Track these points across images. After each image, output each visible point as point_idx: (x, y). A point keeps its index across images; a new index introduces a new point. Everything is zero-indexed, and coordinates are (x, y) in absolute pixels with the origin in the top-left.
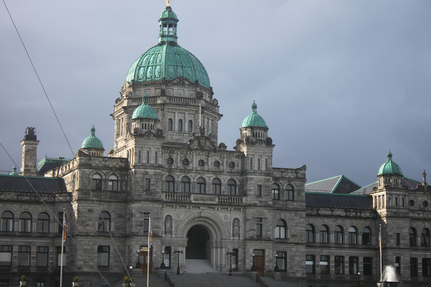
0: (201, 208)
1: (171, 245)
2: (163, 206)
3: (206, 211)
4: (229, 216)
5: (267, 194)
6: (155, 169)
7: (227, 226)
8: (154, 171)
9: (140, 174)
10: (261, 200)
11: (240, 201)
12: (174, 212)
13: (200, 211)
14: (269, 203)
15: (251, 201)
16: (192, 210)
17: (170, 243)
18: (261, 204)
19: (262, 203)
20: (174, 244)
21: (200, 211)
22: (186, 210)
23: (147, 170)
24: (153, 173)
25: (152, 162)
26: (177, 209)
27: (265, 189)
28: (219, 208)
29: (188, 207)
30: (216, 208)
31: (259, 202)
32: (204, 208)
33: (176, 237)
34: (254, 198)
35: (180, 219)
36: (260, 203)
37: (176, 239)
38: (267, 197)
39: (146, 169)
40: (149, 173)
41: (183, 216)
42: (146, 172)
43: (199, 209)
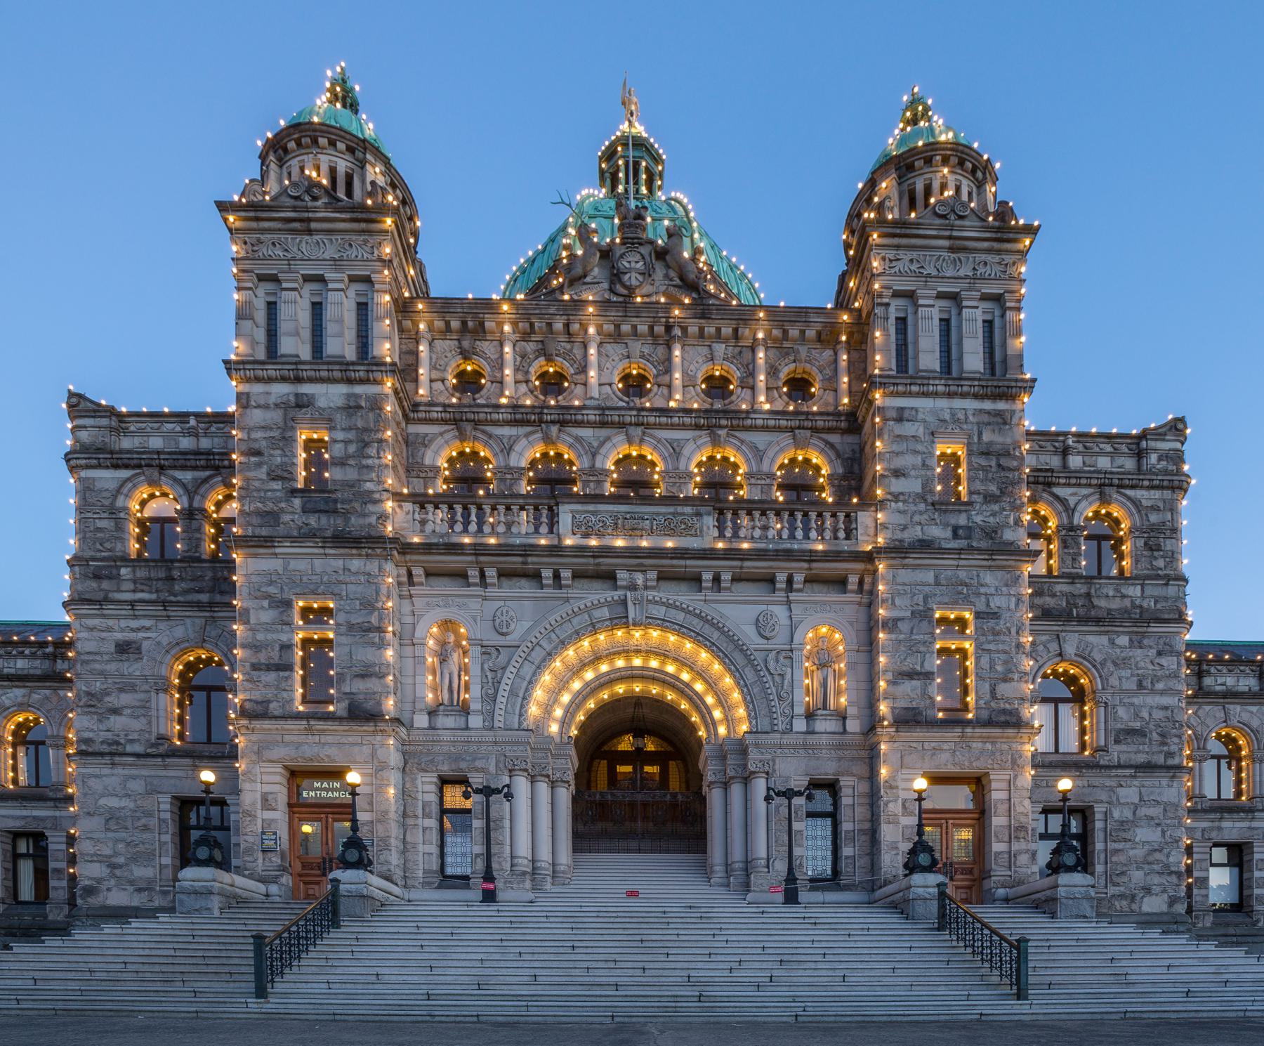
0: (622, 575)
1: (463, 765)
2: (410, 575)
3: (651, 594)
4: (784, 621)
5: (993, 488)
6: (350, 381)
7: (772, 665)
8: (343, 389)
9: (266, 407)
10: (962, 520)
11: (842, 534)
12: (474, 604)
13: (617, 594)
14: (1008, 535)
15: (905, 528)
16: (572, 593)
17: (458, 758)
18: (962, 543)
19: (969, 537)
20: (479, 764)
21: (617, 594)
22: (539, 593)
23: (306, 389)
24: (340, 402)
25: (341, 344)
26: (491, 591)
27: (984, 462)
28: (726, 576)
29: (547, 574)
30: (707, 576)
31: (948, 533)
32: (639, 579)
33: (492, 728)
34: (921, 513)
35: (509, 640)
36: (955, 535)
37: (489, 736)
38: (996, 507)
39: (298, 380)
40: (322, 403)
41: (527, 625)
42: (297, 395)
43: (616, 588)
